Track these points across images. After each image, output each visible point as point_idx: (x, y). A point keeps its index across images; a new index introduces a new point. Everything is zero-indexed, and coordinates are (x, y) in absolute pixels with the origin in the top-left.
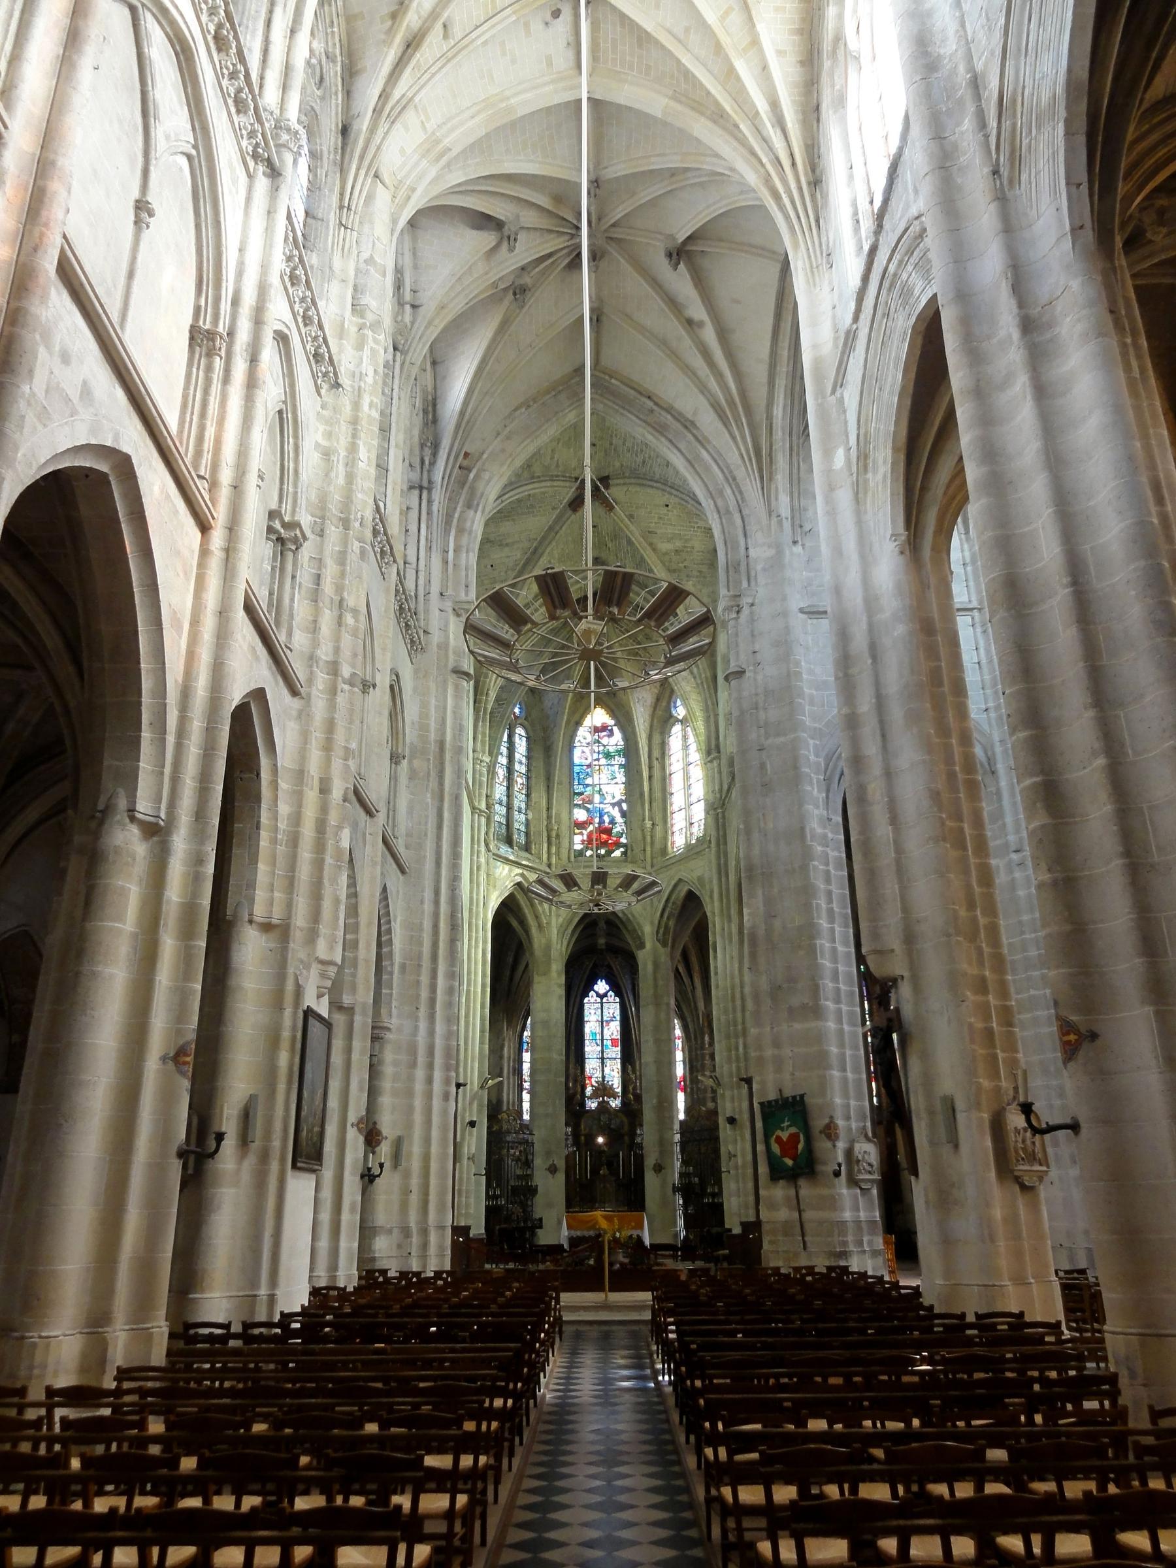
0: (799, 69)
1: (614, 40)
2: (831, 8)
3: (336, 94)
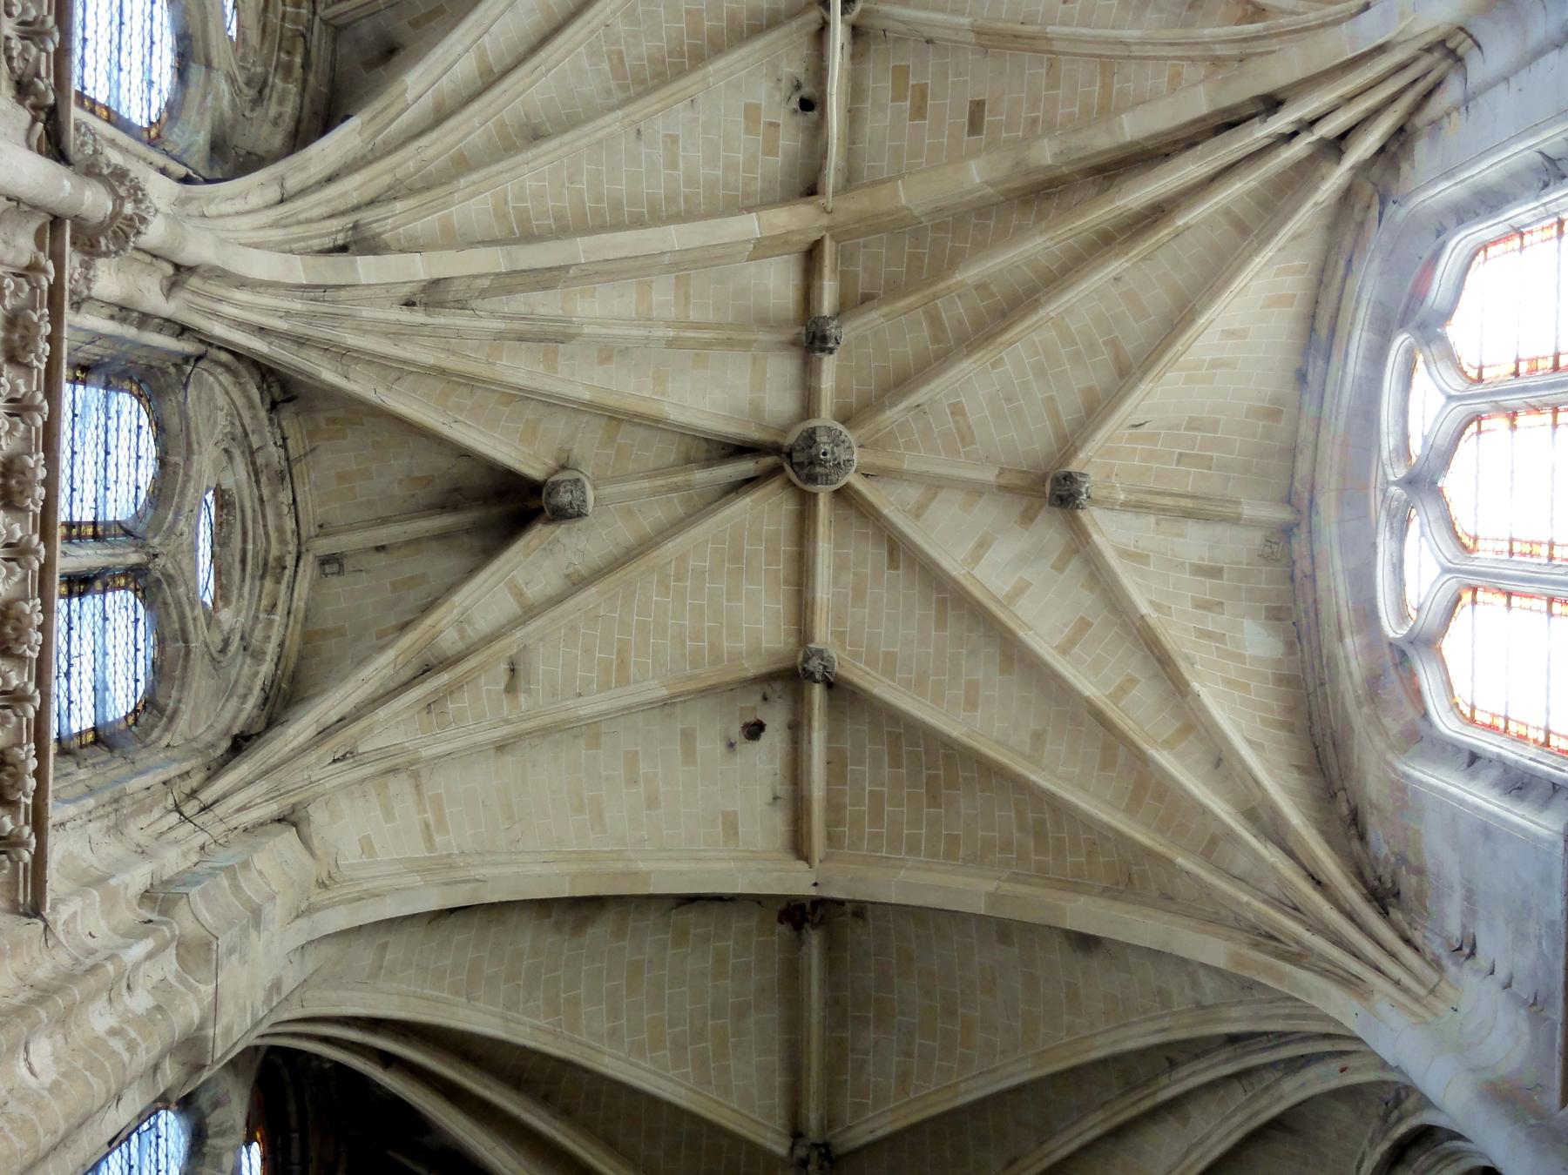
0: (1296, 775)
1: (876, 798)
2: (1348, 641)
3: (245, 697)
